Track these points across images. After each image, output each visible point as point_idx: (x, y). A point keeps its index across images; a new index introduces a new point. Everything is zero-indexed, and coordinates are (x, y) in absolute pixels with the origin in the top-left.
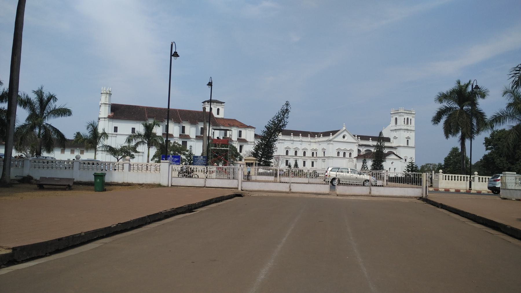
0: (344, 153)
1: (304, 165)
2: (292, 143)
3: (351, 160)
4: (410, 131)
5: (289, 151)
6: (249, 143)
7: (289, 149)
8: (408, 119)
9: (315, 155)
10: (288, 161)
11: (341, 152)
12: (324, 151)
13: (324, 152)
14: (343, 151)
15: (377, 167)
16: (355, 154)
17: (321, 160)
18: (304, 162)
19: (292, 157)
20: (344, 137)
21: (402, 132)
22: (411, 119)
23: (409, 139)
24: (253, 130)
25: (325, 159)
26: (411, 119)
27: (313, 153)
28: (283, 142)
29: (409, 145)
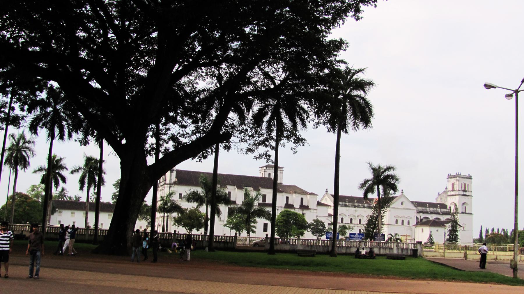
2: (348, 210)
4: (467, 197)
6: (312, 211)
8: (465, 184)
15: (452, 237)
16: (413, 222)
20: (402, 204)
22: (468, 185)
24: (315, 196)
26: (468, 185)
29: (467, 212)
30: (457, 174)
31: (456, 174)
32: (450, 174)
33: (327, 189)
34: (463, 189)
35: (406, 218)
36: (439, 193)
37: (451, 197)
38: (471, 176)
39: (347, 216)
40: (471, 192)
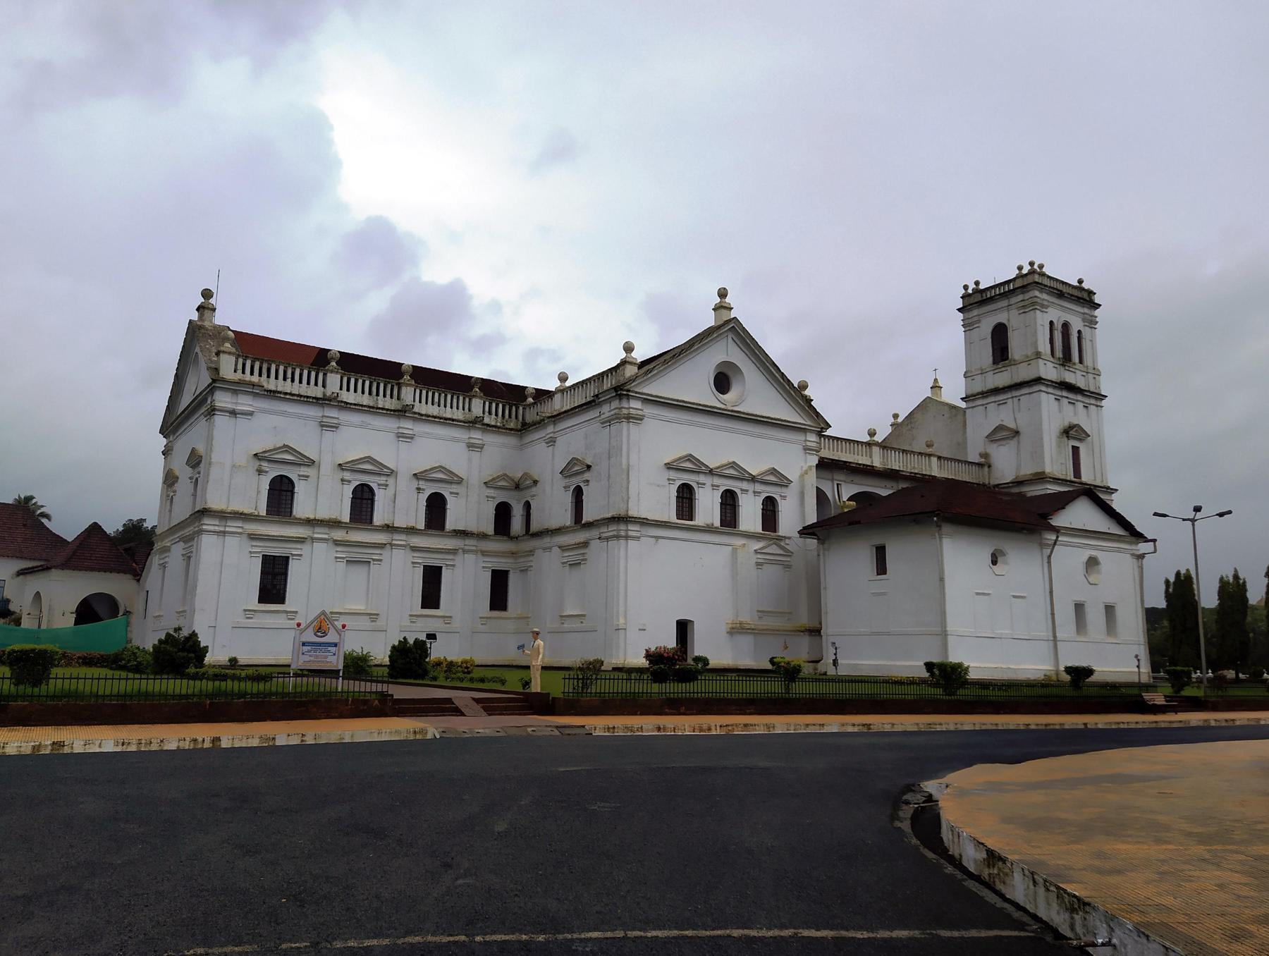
0: (729, 502)
1: (431, 597)
3: (774, 549)
4: (1079, 397)
5: (300, 489)
7: (304, 471)
8: (1066, 326)
9: (517, 525)
10: (285, 560)
11: (701, 485)
12: (576, 481)
13: (578, 493)
14: (717, 481)
17: (556, 550)
18: (432, 578)
19: (320, 533)
20: (722, 382)
21: (1047, 401)
22: (1079, 332)
23: (1081, 440)
25: (585, 544)
26: (1079, 332)
27: (503, 512)
28: (244, 403)
30: (1025, 271)
31: (1013, 274)
32: (977, 283)
33: (207, 294)
34: (1059, 353)
35: (753, 479)
36: (896, 416)
37: (992, 399)
38: (1091, 293)
39: (327, 467)
40: (1097, 374)
